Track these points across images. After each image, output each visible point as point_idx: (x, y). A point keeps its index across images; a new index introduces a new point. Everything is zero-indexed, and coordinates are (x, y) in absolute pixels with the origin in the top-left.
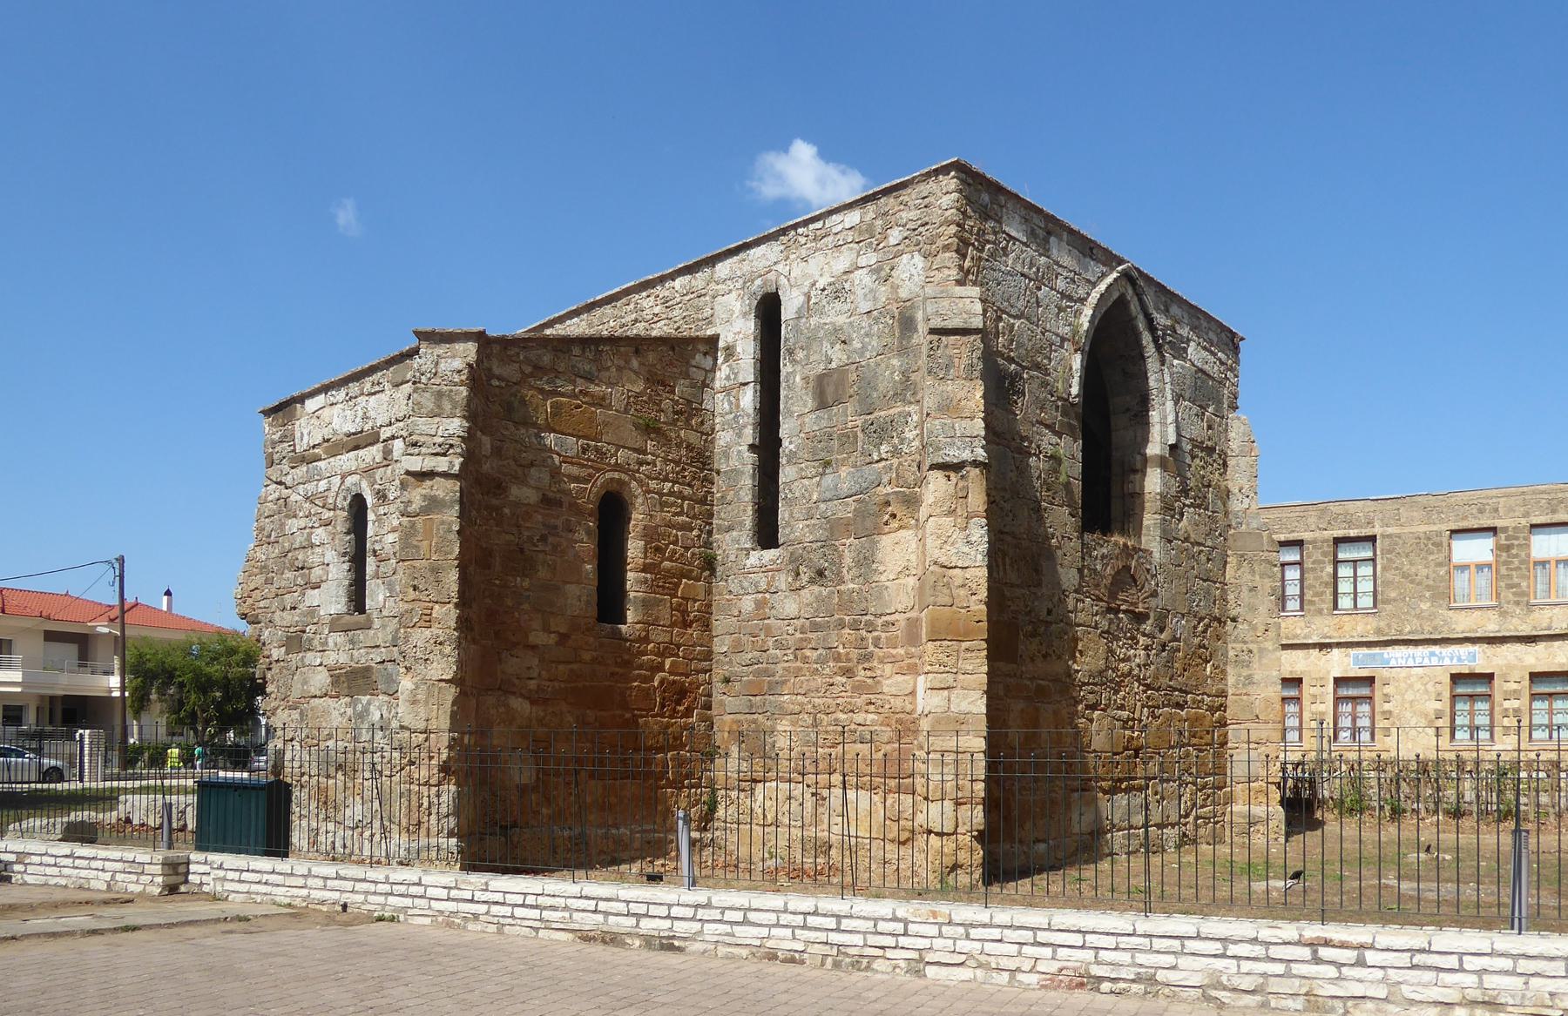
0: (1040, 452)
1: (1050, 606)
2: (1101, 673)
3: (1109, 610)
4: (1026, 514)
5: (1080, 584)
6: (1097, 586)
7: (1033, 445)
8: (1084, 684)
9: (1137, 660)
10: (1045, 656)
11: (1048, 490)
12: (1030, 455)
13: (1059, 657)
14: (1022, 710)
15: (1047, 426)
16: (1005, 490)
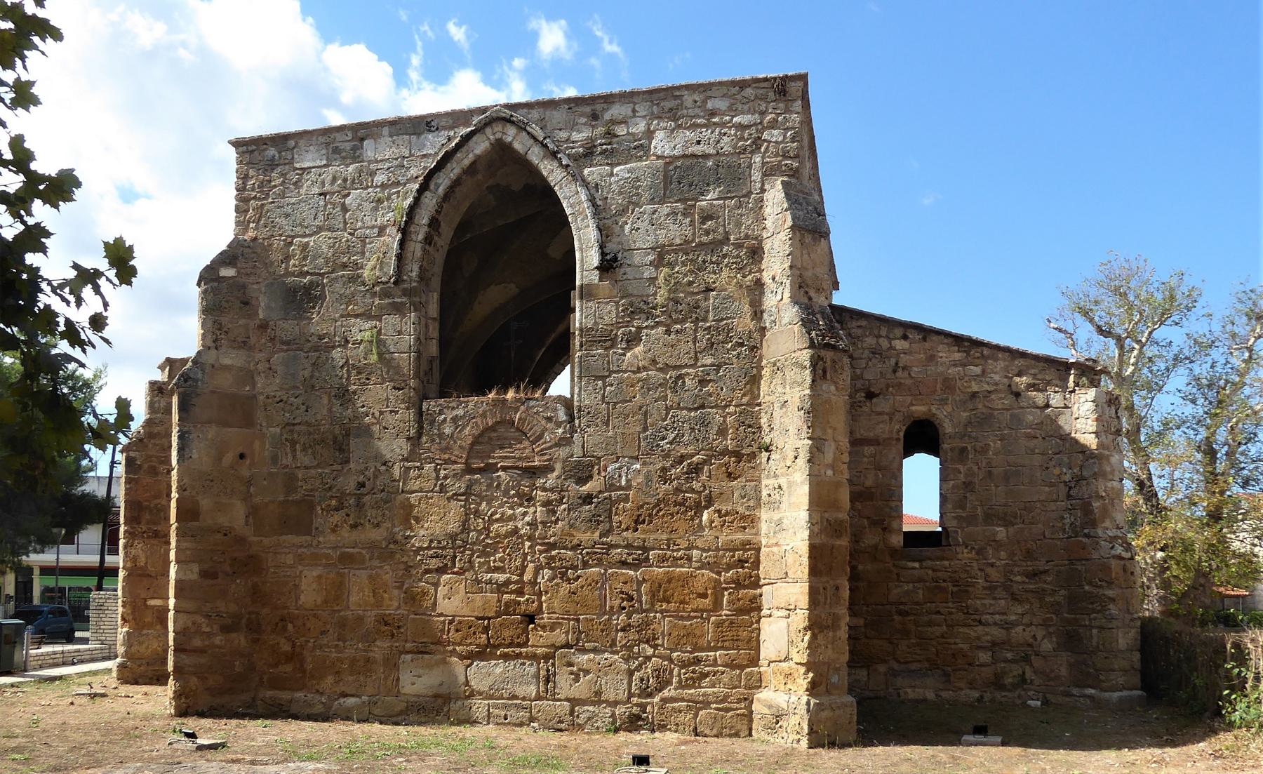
0: (347, 342)
1: (361, 479)
2: (453, 537)
3: (469, 470)
4: (325, 400)
5: (412, 452)
6: (446, 449)
7: (337, 339)
8: (421, 549)
9: (528, 519)
10: (354, 526)
11: (359, 373)
12: (334, 347)
13: (378, 525)
14: (319, 577)
15: (356, 316)
16: (298, 387)
